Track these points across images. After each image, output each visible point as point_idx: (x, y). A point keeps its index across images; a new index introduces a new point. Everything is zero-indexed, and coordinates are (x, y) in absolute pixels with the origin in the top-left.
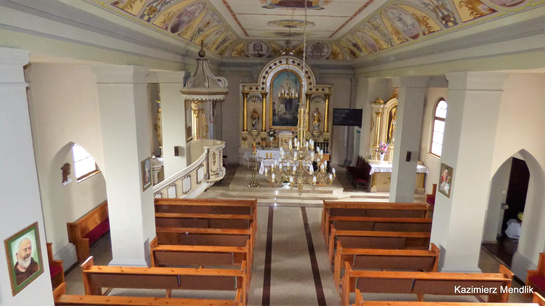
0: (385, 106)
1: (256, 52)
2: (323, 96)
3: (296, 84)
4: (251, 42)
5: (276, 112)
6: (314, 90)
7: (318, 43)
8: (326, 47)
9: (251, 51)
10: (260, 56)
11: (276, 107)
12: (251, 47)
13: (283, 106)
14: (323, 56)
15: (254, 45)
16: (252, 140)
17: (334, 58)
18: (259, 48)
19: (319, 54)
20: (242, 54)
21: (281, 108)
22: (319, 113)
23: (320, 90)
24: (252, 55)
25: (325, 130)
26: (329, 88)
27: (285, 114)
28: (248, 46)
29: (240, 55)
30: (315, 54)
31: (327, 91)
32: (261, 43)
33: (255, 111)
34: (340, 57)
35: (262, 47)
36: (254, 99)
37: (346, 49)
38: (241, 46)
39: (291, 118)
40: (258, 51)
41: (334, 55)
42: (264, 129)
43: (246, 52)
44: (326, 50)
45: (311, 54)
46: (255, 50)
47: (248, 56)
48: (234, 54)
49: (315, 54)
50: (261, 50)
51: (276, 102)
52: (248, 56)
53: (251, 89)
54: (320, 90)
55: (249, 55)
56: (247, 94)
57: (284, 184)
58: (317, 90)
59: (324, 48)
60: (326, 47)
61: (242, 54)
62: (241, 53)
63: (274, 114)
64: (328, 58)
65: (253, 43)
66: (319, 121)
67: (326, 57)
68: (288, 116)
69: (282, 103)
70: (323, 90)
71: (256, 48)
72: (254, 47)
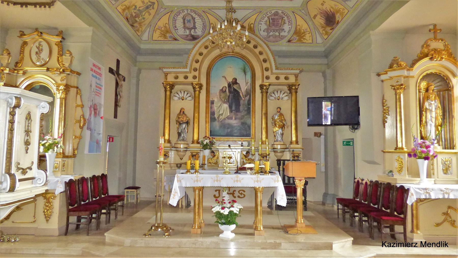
0: (411, 73)
1: (188, 32)
2: (286, 88)
3: (245, 72)
4: (179, 13)
5: (216, 116)
6: (273, 79)
7: (276, 14)
8: (287, 21)
9: (181, 31)
10: (194, 38)
11: (215, 108)
12: (179, 23)
13: (226, 106)
14: (283, 37)
15: (184, 19)
16: (178, 158)
17: (300, 40)
18: (192, 26)
19: (277, 34)
20: (168, 35)
21: (223, 110)
22: (281, 115)
23: (282, 80)
24: (181, 36)
25: (294, 139)
26: (296, 76)
27: (229, 118)
28: (175, 20)
29: (165, 37)
30: (271, 34)
31: (292, 80)
32: (194, 15)
33: (182, 112)
34: (308, 36)
35: (194, 23)
36: (181, 95)
37: (319, 16)
38: (165, 20)
39: (240, 124)
40: (190, 29)
41: (299, 34)
42: (196, 138)
43: (173, 32)
44: (286, 27)
45: (265, 34)
46: (185, 27)
47: (176, 39)
48: (156, 36)
49: (271, 34)
50: (195, 28)
51: (216, 100)
52: (176, 39)
53: (176, 78)
54: (282, 80)
55: (178, 38)
56: (172, 86)
57: (222, 227)
58: (277, 78)
59: (284, 23)
60: (287, 21)
61: (168, 35)
62: (165, 33)
63: (213, 119)
64: (289, 41)
65: (182, 15)
66: (283, 127)
67: (287, 39)
68: (234, 122)
69: (224, 102)
70: (286, 78)
71: (187, 25)
72: (184, 23)
